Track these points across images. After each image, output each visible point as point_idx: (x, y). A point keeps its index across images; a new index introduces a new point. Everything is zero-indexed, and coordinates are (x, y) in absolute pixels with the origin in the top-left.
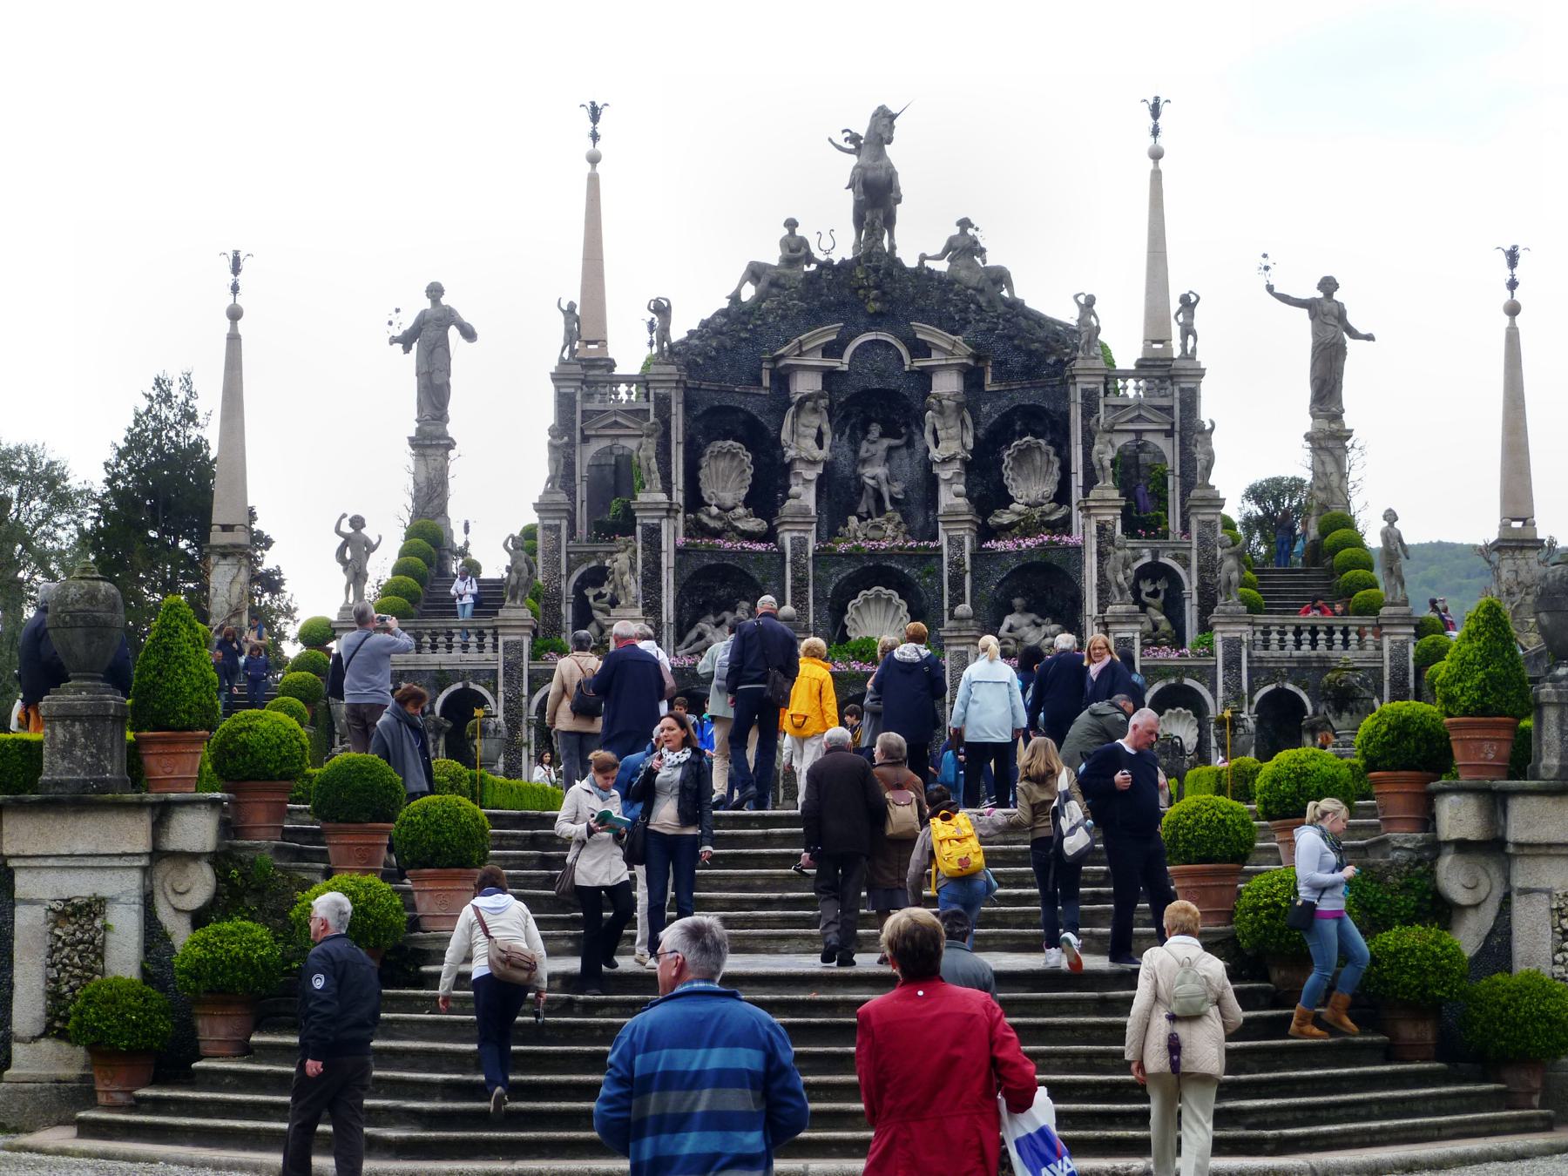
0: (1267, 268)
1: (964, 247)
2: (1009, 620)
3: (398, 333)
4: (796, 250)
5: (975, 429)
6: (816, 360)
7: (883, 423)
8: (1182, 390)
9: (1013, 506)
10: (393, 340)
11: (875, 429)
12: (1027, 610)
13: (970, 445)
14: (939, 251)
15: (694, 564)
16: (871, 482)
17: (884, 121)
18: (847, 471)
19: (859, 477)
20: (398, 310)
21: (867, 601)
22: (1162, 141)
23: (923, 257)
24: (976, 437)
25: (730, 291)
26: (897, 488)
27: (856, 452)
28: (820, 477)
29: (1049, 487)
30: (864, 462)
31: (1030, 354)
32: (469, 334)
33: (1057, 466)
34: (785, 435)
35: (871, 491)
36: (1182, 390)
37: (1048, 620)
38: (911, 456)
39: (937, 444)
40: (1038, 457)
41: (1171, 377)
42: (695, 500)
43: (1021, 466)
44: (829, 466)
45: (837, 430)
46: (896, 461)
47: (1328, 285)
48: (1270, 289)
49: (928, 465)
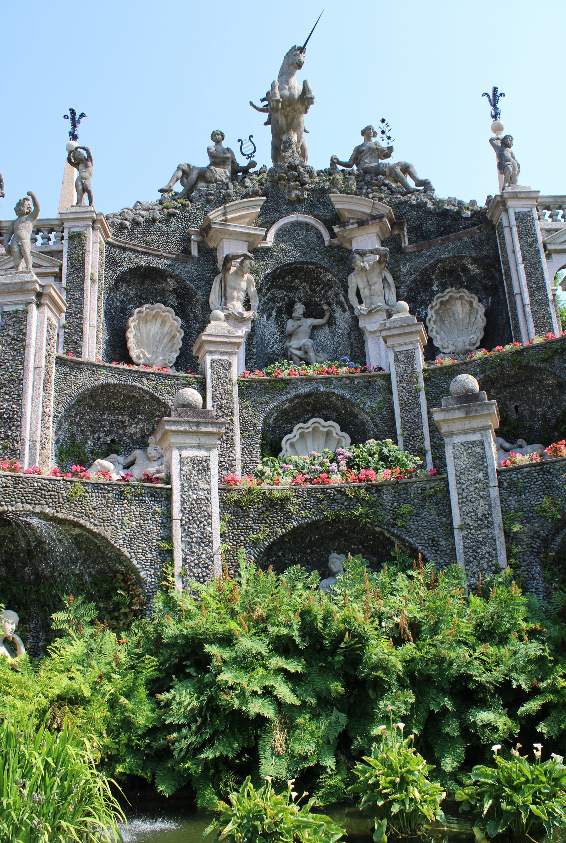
5: (397, 288)
7: (305, 304)
11: (299, 309)
14: (345, 157)
15: (85, 381)
18: (276, 349)
21: (302, 435)
23: (334, 162)
25: (163, 186)
28: (250, 337)
30: (290, 336)
31: (445, 213)
33: (481, 310)
34: (214, 297)
38: (333, 334)
39: (361, 302)
40: (460, 309)
43: (442, 321)
45: (264, 310)
46: (319, 339)
49: (356, 320)
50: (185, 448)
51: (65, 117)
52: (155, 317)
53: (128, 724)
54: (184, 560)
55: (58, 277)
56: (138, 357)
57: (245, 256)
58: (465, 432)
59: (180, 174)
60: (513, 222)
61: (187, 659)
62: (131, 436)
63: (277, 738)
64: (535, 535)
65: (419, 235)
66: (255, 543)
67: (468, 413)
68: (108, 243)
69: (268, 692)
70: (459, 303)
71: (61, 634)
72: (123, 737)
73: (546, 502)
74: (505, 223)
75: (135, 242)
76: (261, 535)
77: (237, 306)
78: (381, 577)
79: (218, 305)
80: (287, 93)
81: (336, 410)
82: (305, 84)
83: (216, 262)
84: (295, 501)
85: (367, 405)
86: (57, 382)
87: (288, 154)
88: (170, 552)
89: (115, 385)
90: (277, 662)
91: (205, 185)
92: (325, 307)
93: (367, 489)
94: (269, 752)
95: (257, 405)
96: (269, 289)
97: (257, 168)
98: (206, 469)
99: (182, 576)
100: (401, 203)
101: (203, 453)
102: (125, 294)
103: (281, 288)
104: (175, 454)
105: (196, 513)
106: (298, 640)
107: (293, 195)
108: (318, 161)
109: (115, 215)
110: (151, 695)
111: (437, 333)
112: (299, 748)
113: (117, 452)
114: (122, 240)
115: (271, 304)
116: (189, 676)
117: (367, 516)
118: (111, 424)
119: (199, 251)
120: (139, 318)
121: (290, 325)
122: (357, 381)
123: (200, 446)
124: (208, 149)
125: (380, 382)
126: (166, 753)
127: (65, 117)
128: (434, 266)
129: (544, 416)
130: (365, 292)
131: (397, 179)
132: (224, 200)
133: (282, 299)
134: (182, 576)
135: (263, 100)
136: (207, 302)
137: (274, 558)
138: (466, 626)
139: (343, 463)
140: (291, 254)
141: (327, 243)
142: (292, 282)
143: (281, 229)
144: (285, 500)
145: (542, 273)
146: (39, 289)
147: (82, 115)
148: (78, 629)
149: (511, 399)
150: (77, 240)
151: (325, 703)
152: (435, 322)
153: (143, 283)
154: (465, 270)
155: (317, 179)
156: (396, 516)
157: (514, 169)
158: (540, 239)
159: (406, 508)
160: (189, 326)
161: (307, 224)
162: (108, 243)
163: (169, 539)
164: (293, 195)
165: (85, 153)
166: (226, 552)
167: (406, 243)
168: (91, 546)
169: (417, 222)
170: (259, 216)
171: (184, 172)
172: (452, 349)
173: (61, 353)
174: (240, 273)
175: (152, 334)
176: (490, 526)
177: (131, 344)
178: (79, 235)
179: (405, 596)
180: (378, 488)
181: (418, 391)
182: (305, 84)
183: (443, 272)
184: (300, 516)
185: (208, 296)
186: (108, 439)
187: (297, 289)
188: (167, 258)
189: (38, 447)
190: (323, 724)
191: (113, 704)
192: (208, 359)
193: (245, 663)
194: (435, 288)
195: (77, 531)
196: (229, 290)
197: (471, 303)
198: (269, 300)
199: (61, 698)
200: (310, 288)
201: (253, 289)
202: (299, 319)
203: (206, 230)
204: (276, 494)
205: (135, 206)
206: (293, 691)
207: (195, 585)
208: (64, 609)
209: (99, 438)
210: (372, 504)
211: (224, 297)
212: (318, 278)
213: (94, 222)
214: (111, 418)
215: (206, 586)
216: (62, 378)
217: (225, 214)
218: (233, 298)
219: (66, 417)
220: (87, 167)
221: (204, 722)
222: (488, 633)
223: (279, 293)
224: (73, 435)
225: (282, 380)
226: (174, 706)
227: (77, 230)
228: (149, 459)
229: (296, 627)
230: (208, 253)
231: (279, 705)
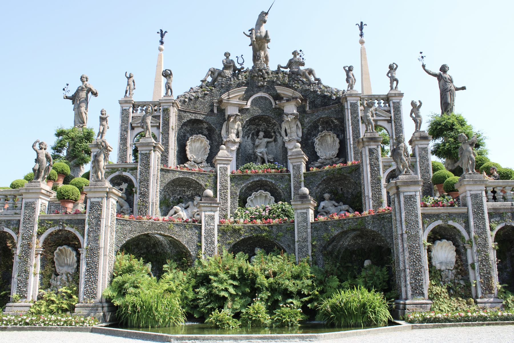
0: (422, 57)
1: (295, 62)
2: (322, 204)
3: (70, 94)
4: (228, 65)
6: (235, 101)
7: (265, 132)
8: (394, 103)
9: (319, 160)
10: (67, 98)
11: (261, 134)
12: (331, 199)
13: (300, 135)
14: (285, 65)
15: (171, 177)
16: (260, 154)
17: (262, 19)
18: (251, 152)
19: (255, 153)
20: (68, 85)
21: (255, 197)
22: (364, 38)
23: (279, 67)
24: (303, 133)
25: (202, 79)
26: (271, 157)
27: (254, 144)
28: (238, 149)
29: (335, 152)
30: (257, 146)
31: (325, 96)
32: (95, 94)
33: (338, 141)
34: (223, 132)
35: (260, 158)
36: (394, 103)
37: (341, 203)
38: (276, 145)
39: (286, 135)
40: (329, 139)
43: (322, 144)
44: (240, 144)
45: (246, 134)
46: (270, 148)
47: (444, 69)
48: (424, 66)
49: (284, 143)
50: (206, 211)
51: (158, 33)
52: (198, 140)
53: (186, 298)
54: (205, 249)
55: (158, 127)
56: (191, 158)
57: (237, 115)
58: (301, 209)
59: (210, 73)
60: (349, 107)
61: (204, 280)
62: (187, 196)
63: (230, 304)
64: (321, 245)
65: (313, 105)
66: (229, 244)
67: (302, 203)
68: (179, 110)
69: (226, 290)
70: (329, 137)
71: (166, 271)
72: (185, 301)
73: (325, 235)
74: (346, 107)
75: (191, 108)
76: (231, 241)
77: (233, 136)
78: (269, 257)
79: (225, 135)
80: (259, 34)
81: (270, 186)
82: (267, 31)
83: (225, 115)
84: (243, 230)
85: (281, 186)
86: (160, 178)
87: (259, 62)
88: (201, 246)
89: (182, 178)
90: (231, 282)
92: (273, 134)
93: (268, 227)
94: (226, 307)
95: (237, 185)
96: (248, 126)
97: (245, 69)
98: (213, 219)
99: (204, 254)
100: (306, 90)
101: (212, 213)
102: (185, 130)
103: (254, 125)
104: (203, 214)
105: (210, 234)
106: (237, 276)
107: (260, 84)
108: (272, 67)
109: (181, 96)
110: (193, 290)
111: (319, 149)
112: (235, 307)
113: (182, 202)
114: (184, 108)
115: (249, 132)
116: (205, 285)
117: (267, 236)
118: (180, 191)
119: (217, 110)
120: (191, 141)
121: (257, 141)
122: (277, 176)
123: (211, 211)
124: (223, 61)
125: (287, 177)
126: (197, 306)
127: (158, 33)
128: (319, 120)
129: (352, 193)
130: (288, 131)
131: (306, 77)
132: (228, 88)
133: (254, 129)
134: (204, 254)
135: (249, 31)
136: (221, 134)
137: (234, 249)
138: (289, 274)
139: (267, 211)
140: (258, 112)
141: (273, 107)
142: (258, 122)
143: (254, 99)
144: (240, 229)
145: (359, 131)
146: (154, 145)
147: (166, 32)
148: (171, 270)
149: (339, 185)
150: (166, 111)
151: (244, 295)
152: (318, 145)
153: (193, 125)
154: (333, 122)
155: (271, 76)
156: (277, 236)
157: (352, 82)
158: (360, 115)
159: (280, 234)
160: (213, 143)
161: (266, 97)
162: (179, 110)
163: (200, 242)
164: (260, 84)
165: (169, 72)
166: (219, 246)
167: (307, 109)
168: (175, 244)
169: (313, 99)
170: (244, 94)
171: (212, 72)
172: (324, 157)
173: (162, 167)
174: (235, 121)
175: (197, 147)
176: (307, 241)
177: (188, 152)
178: (167, 109)
179: (275, 263)
180: (272, 226)
181: (301, 182)
182: (267, 31)
183: (323, 122)
184: (245, 235)
185: (221, 131)
186: (179, 197)
187: (261, 125)
188: (203, 115)
189: (155, 204)
190: (243, 301)
191: (182, 292)
192: (219, 166)
193: (221, 282)
194: (320, 129)
195: (171, 239)
196: (230, 129)
197: (334, 137)
198: (248, 130)
199: (167, 290)
200: (267, 125)
201: (240, 128)
202: (261, 139)
203: (220, 101)
204: (237, 227)
205: (190, 90)
206: (235, 291)
207: (208, 257)
208: (166, 263)
209: (175, 197)
210: (269, 232)
211: (228, 132)
212: (270, 121)
213: (173, 103)
214: (180, 189)
215: (213, 257)
216: (162, 176)
217: (228, 96)
218: (231, 133)
219: (163, 190)
220: (170, 78)
221: (208, 298)
222: (297, 277)
223: (253, 127)
224: (165, 196)
225: (248, 175)
226: (200, 293)
227: (166, 107)
228: (194, 206)
229: (237, 272)
230: (222, 111)
231: (231, 295)
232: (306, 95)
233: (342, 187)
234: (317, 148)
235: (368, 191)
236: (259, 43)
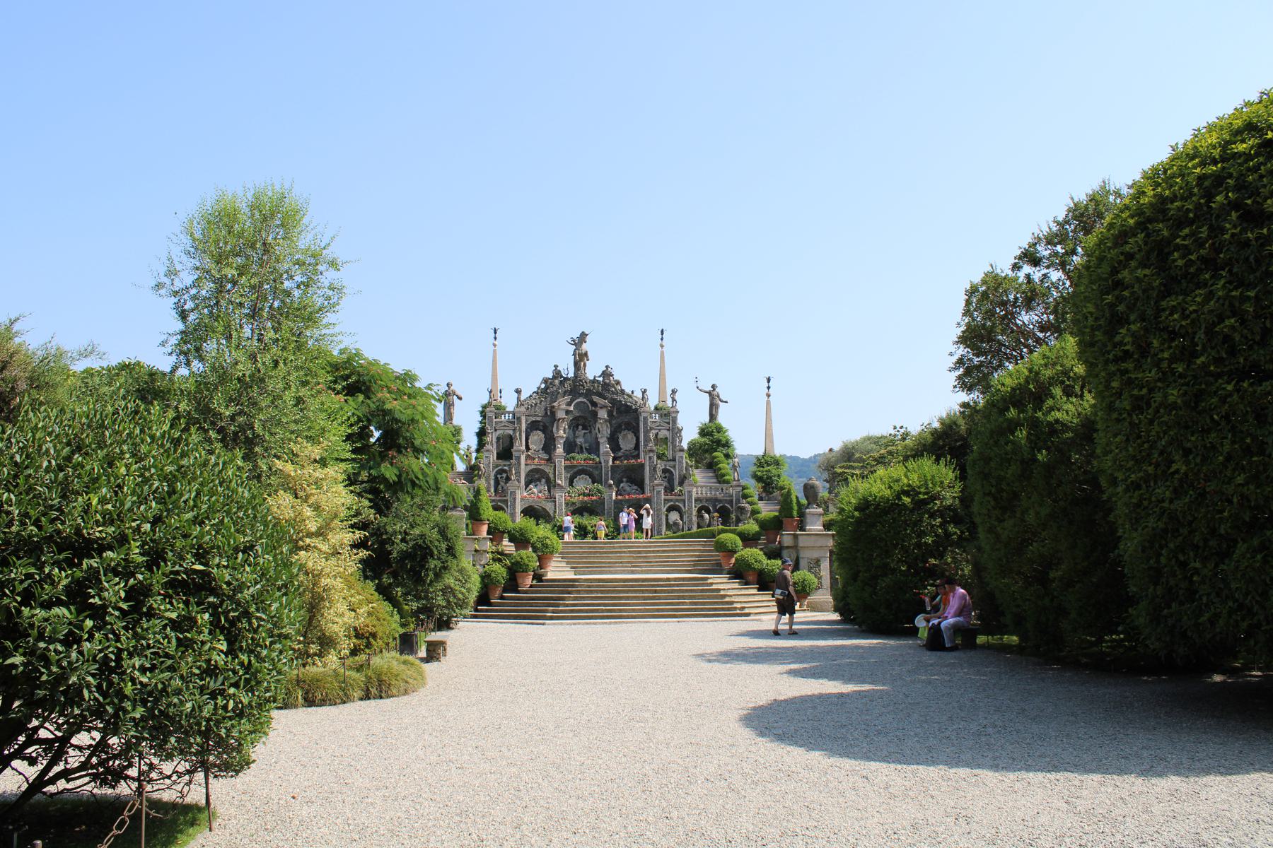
1: (606, 374)
4: (557, 374)
6: (564, 407)
17: (583, 337)
29: (633, 446)
32: (460, 398)
41: (668, 415)
42: (528, 448)
47: (713, 386)
65: (619, 411)
91: (552, 387)
184: (578, 505)
211: (558, 429)
232: (613, 402)
233: (634, 476)
234: (621, 441)
235: (647, 481)
236: (580, 359)
